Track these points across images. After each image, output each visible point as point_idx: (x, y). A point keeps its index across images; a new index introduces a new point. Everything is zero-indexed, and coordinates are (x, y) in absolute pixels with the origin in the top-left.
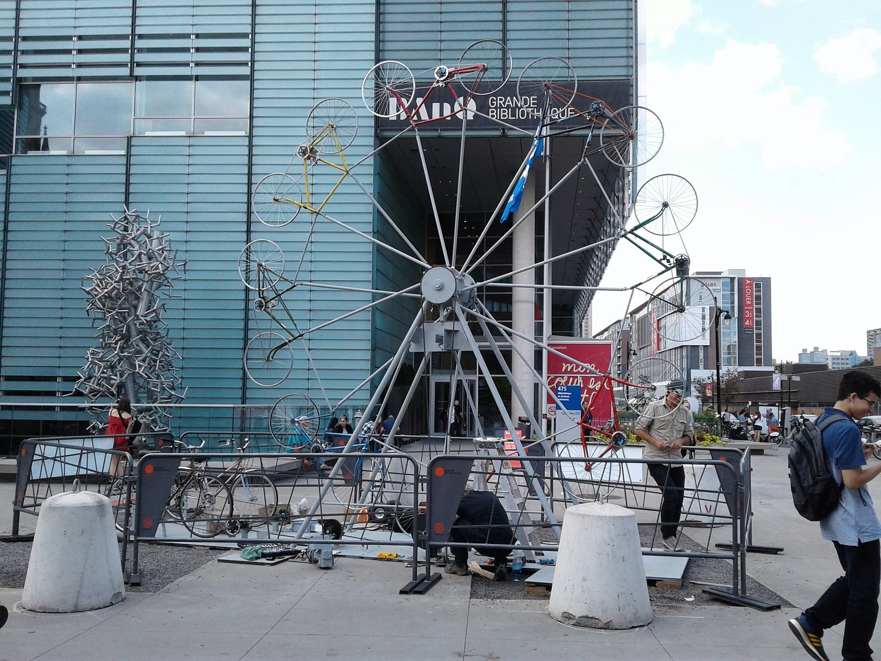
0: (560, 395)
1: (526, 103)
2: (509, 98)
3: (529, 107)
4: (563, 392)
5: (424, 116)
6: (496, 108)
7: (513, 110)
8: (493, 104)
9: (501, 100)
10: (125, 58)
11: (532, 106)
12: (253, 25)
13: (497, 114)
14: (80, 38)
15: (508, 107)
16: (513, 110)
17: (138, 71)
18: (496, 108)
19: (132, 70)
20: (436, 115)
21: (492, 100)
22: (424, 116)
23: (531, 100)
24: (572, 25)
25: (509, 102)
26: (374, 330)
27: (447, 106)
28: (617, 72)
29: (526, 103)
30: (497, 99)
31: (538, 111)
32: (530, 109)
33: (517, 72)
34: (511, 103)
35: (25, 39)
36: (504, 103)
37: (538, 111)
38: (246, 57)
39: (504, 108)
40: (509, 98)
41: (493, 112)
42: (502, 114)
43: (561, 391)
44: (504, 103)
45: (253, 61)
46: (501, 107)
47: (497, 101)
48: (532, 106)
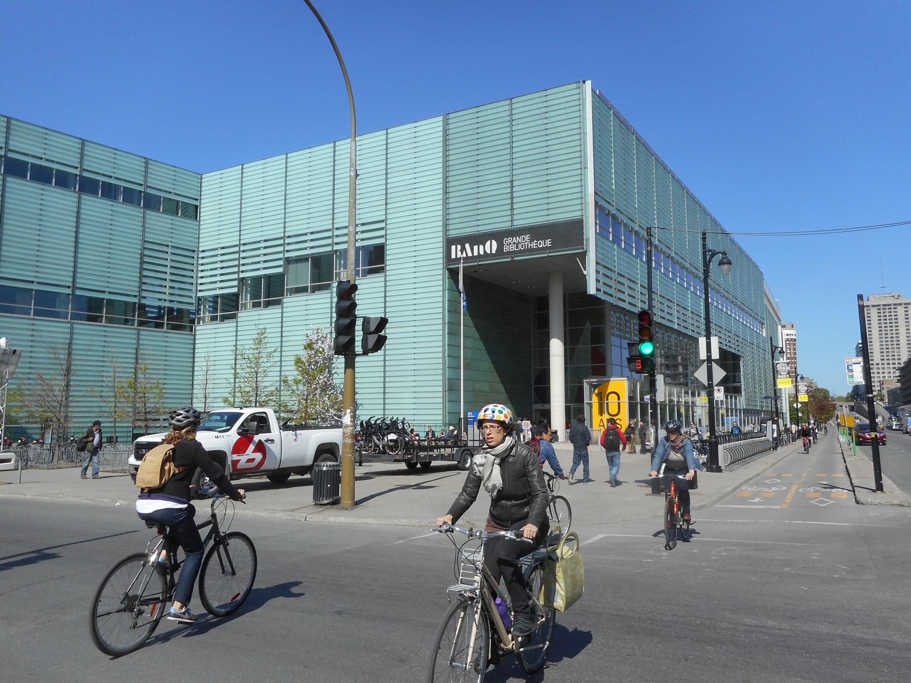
3: (526, 242)
6: (508, 245)
7: (517, 245)
12: (386, 214)
14: (312, 233)
16: (517, 245)
18: (508, 245)
20: (476, 254)
22: (470, 254)
23: (527, 237)
24: (550, 189)
27: (481, 247)
28: (576, 215)
31: (531, 244)
32: (526, 243)
33: (519, 223)
35: (289, 237)
37: (531, 244)
38: (382, 233)
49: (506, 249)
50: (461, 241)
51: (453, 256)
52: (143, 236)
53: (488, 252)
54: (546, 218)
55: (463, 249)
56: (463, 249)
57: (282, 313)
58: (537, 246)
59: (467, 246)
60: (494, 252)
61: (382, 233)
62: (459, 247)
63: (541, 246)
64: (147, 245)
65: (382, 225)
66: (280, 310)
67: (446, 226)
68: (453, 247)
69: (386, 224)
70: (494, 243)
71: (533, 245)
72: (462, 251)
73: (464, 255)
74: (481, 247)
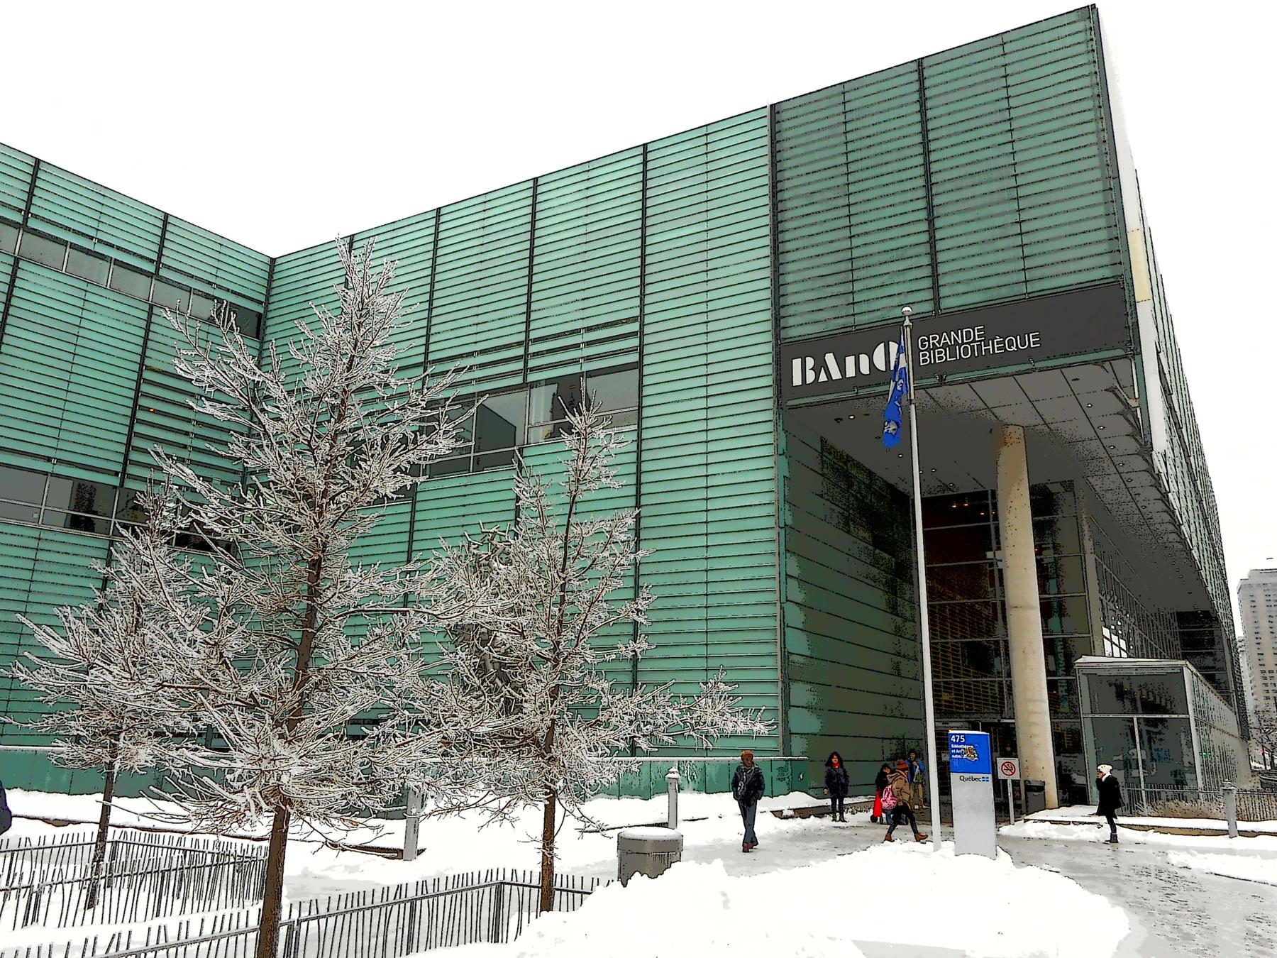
0: (956, 749)
1: (968, 337)
3: (974, 341)
4: (959, 743)
5: (836, 375)
8: (923, 346)
9: (934, 338)
10: (519, 365)
11: (977, 339)
13: (930, 357)
15: (945, 346)
17: (532, 377)
19: (525, 378)
20: (851, 372)
21: (923, 341)
22: (836, 375)
25: (945, 339)
26: (786, 655)
27: (864, 359)
29: (968, 337)
30: (929, 338)
32: (975, 344)
34: (948, 341)
36: (939, 343)
38: (634, 342)
39: (940, 348)
40: (945, 334)
41: (924, 355)
42: (937, 356)
43: (956, 743)
44: (939, 342)
45: (642, 345)
46: (935, 347)
47: (929, 341)
48: (977, 339)
50: (814, 347)
51: (797, 381)
52: (143, 356)
54: (1022, 289)
55: (820, 366)
56: (820, 366)
57: (413, 512)
59: (830, 359)
61: (634, 342)
62: (810, 362)
63: (1014, 348)
64: (147, 375)
65: (635, 327)
66: (408, 508)
67: (777, 319)
68: (797, 363)
69: (642, 326)
71: (994, 346)
72: (816, 370)
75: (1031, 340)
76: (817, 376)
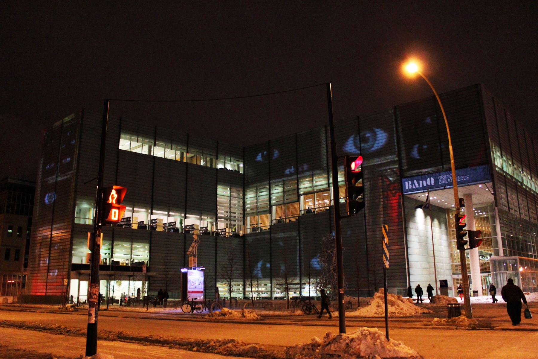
2: (445, 176)
5: (417, 186)
6: (441, 180)
15: (445, 178)
18: (441, 180)
20: (421, 186)
22: (417, 186)
27: (424, 182)
29: (451, 176)
46: (443, 179)
49: (441, 182)
51: (407, 188)
53: (429, 183)
55: (413, 184)
56: (413, 184)
58: (460, 180)
59: (415, 182)
60: (432, 184)
62: (410, 183)
63: (463, 180)
68: (406, 183)
70: (432, 179)
72: (412, 184)
73: (414, 187)
74: (424, 182)
75: (467, 178)
76: (412, 186)
